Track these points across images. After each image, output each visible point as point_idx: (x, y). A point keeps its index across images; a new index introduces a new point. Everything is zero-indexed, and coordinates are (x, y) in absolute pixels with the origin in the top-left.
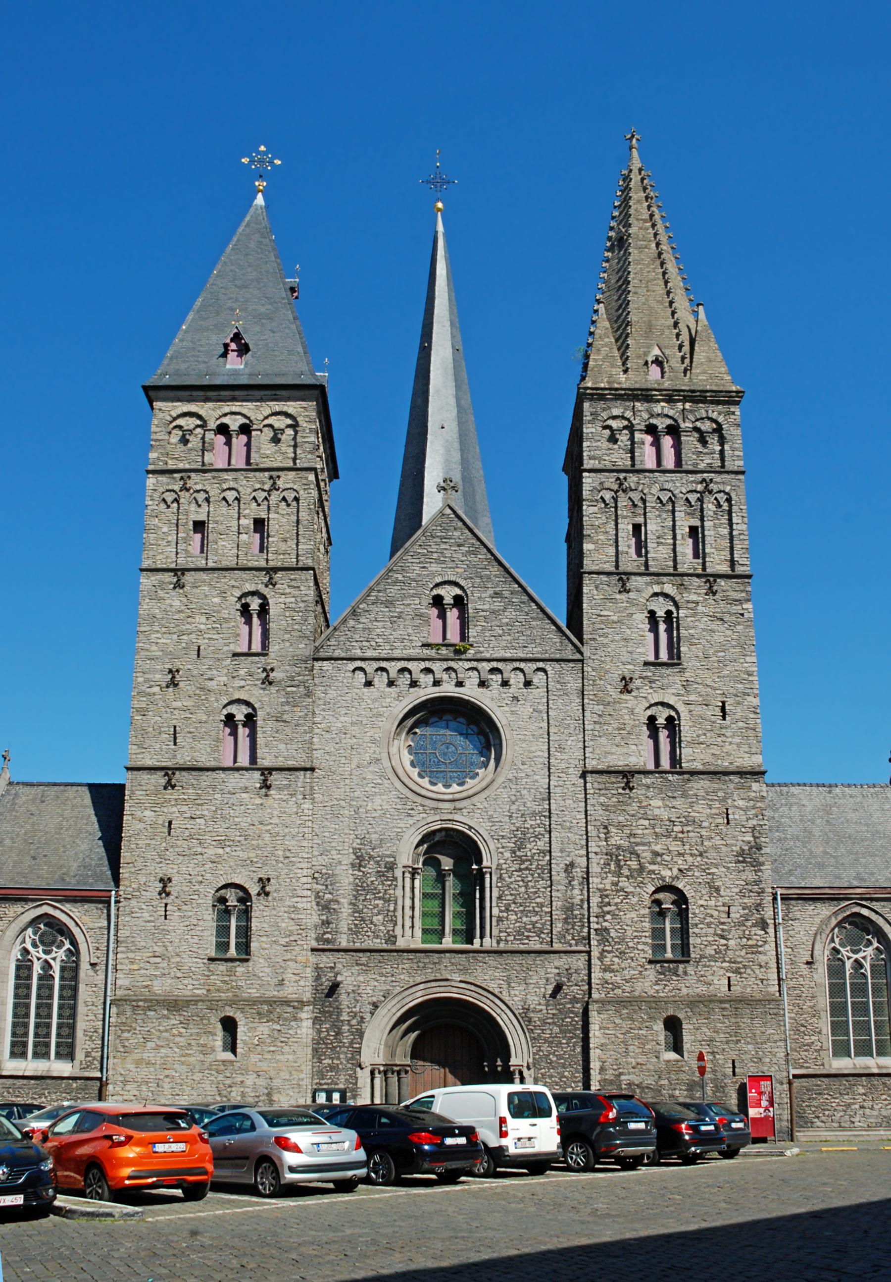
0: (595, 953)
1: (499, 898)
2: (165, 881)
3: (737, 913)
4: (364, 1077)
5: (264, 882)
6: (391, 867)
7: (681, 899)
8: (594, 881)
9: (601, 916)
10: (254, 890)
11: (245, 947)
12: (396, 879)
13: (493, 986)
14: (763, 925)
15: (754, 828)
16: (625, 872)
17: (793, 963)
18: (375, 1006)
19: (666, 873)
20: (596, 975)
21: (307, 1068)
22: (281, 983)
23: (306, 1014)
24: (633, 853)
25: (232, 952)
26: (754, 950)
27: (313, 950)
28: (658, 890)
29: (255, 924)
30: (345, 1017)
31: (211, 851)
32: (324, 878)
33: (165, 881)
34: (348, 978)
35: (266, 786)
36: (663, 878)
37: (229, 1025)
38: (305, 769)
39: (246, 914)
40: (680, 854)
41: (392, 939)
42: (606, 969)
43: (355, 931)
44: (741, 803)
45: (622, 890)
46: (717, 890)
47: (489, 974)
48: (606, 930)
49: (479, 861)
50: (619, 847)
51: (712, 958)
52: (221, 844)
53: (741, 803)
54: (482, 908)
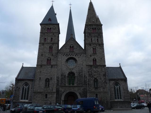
0: (88, 86)
1: (77, 80)
2: (40, 78)
3: (103, 82)
4: (62, 101)
5: (51, 78)
6: (65, 76)
7: (97, 80)
8: (87, 78)
9: (88, 82)
10: (50, 79)
11: (48, 86)
12: (66, 77)
13: (76, 90)
14: (106, 83)
15: (105, 72)
16: (91, 77)
17: (110, 88)
18: (63, 92)
19: (96, 77)
20: (88, 89)
21: (55, 100)
22: (52, 90)
23: (56, 93)
24: (92, 75)
25: (47, 86)
26: (106, 86)
27: (56, 86)
28: (95, 79)
29: (50, 83)
30: (60, 94)
31: (45, 75)
32: (58, 77)
33: (40, 78)
34: (60, 89)
35: (52, 67)
36: (95, 77)
37: (46, 95)
38: (56, 65)
39: (49, 81)
40: (97, 75)
41: (65, 85)
42: (89, 88)
43: (61, 84)
44: (103, 69)
45: (91, 79)
46: (101, 79)
47: (76, 89)
48: (89, 83)
49: (75, 76)
50: (90, 74)
51: (101, 87)
52: (46, 74)
53: (103, 69)
54: (75, 81)
